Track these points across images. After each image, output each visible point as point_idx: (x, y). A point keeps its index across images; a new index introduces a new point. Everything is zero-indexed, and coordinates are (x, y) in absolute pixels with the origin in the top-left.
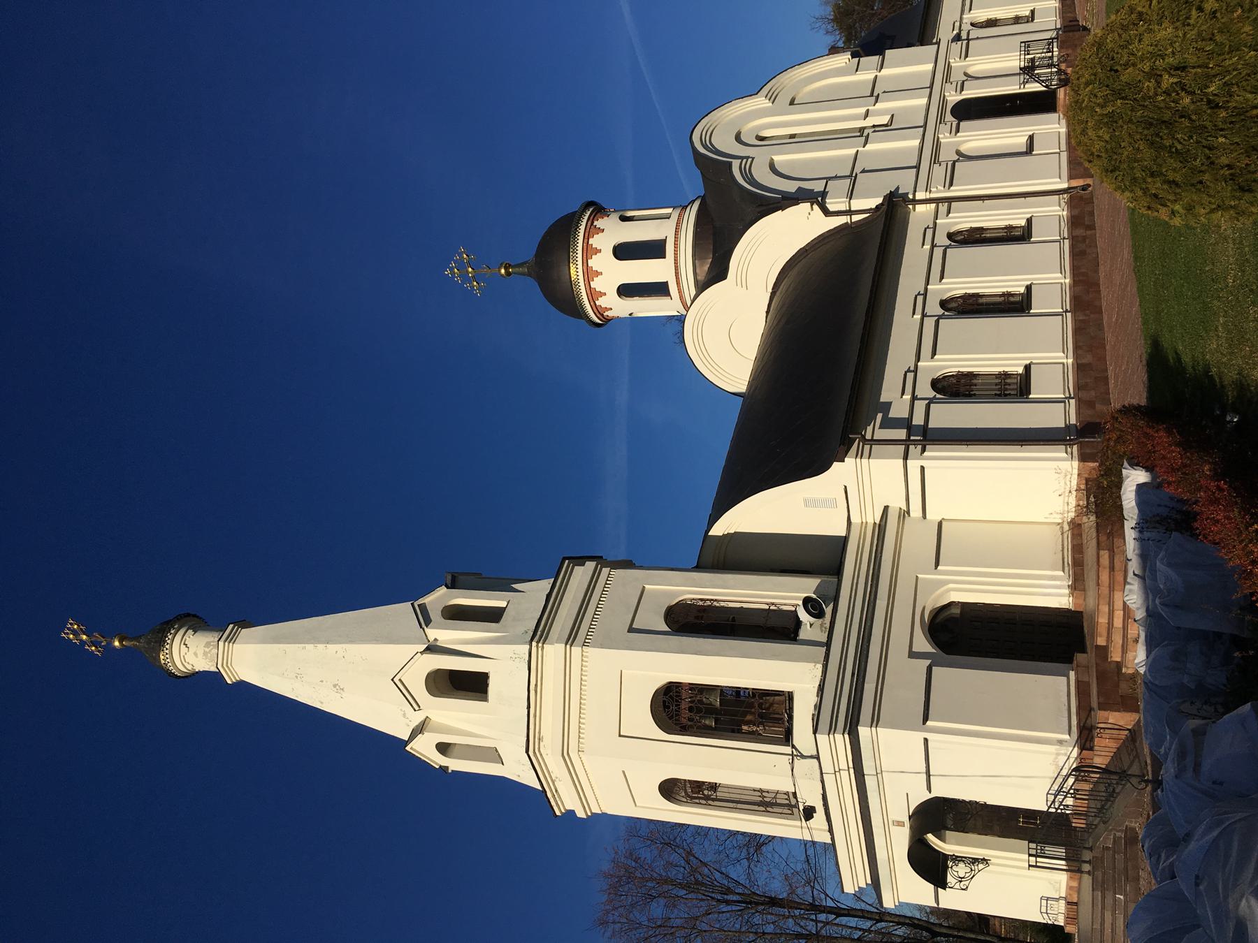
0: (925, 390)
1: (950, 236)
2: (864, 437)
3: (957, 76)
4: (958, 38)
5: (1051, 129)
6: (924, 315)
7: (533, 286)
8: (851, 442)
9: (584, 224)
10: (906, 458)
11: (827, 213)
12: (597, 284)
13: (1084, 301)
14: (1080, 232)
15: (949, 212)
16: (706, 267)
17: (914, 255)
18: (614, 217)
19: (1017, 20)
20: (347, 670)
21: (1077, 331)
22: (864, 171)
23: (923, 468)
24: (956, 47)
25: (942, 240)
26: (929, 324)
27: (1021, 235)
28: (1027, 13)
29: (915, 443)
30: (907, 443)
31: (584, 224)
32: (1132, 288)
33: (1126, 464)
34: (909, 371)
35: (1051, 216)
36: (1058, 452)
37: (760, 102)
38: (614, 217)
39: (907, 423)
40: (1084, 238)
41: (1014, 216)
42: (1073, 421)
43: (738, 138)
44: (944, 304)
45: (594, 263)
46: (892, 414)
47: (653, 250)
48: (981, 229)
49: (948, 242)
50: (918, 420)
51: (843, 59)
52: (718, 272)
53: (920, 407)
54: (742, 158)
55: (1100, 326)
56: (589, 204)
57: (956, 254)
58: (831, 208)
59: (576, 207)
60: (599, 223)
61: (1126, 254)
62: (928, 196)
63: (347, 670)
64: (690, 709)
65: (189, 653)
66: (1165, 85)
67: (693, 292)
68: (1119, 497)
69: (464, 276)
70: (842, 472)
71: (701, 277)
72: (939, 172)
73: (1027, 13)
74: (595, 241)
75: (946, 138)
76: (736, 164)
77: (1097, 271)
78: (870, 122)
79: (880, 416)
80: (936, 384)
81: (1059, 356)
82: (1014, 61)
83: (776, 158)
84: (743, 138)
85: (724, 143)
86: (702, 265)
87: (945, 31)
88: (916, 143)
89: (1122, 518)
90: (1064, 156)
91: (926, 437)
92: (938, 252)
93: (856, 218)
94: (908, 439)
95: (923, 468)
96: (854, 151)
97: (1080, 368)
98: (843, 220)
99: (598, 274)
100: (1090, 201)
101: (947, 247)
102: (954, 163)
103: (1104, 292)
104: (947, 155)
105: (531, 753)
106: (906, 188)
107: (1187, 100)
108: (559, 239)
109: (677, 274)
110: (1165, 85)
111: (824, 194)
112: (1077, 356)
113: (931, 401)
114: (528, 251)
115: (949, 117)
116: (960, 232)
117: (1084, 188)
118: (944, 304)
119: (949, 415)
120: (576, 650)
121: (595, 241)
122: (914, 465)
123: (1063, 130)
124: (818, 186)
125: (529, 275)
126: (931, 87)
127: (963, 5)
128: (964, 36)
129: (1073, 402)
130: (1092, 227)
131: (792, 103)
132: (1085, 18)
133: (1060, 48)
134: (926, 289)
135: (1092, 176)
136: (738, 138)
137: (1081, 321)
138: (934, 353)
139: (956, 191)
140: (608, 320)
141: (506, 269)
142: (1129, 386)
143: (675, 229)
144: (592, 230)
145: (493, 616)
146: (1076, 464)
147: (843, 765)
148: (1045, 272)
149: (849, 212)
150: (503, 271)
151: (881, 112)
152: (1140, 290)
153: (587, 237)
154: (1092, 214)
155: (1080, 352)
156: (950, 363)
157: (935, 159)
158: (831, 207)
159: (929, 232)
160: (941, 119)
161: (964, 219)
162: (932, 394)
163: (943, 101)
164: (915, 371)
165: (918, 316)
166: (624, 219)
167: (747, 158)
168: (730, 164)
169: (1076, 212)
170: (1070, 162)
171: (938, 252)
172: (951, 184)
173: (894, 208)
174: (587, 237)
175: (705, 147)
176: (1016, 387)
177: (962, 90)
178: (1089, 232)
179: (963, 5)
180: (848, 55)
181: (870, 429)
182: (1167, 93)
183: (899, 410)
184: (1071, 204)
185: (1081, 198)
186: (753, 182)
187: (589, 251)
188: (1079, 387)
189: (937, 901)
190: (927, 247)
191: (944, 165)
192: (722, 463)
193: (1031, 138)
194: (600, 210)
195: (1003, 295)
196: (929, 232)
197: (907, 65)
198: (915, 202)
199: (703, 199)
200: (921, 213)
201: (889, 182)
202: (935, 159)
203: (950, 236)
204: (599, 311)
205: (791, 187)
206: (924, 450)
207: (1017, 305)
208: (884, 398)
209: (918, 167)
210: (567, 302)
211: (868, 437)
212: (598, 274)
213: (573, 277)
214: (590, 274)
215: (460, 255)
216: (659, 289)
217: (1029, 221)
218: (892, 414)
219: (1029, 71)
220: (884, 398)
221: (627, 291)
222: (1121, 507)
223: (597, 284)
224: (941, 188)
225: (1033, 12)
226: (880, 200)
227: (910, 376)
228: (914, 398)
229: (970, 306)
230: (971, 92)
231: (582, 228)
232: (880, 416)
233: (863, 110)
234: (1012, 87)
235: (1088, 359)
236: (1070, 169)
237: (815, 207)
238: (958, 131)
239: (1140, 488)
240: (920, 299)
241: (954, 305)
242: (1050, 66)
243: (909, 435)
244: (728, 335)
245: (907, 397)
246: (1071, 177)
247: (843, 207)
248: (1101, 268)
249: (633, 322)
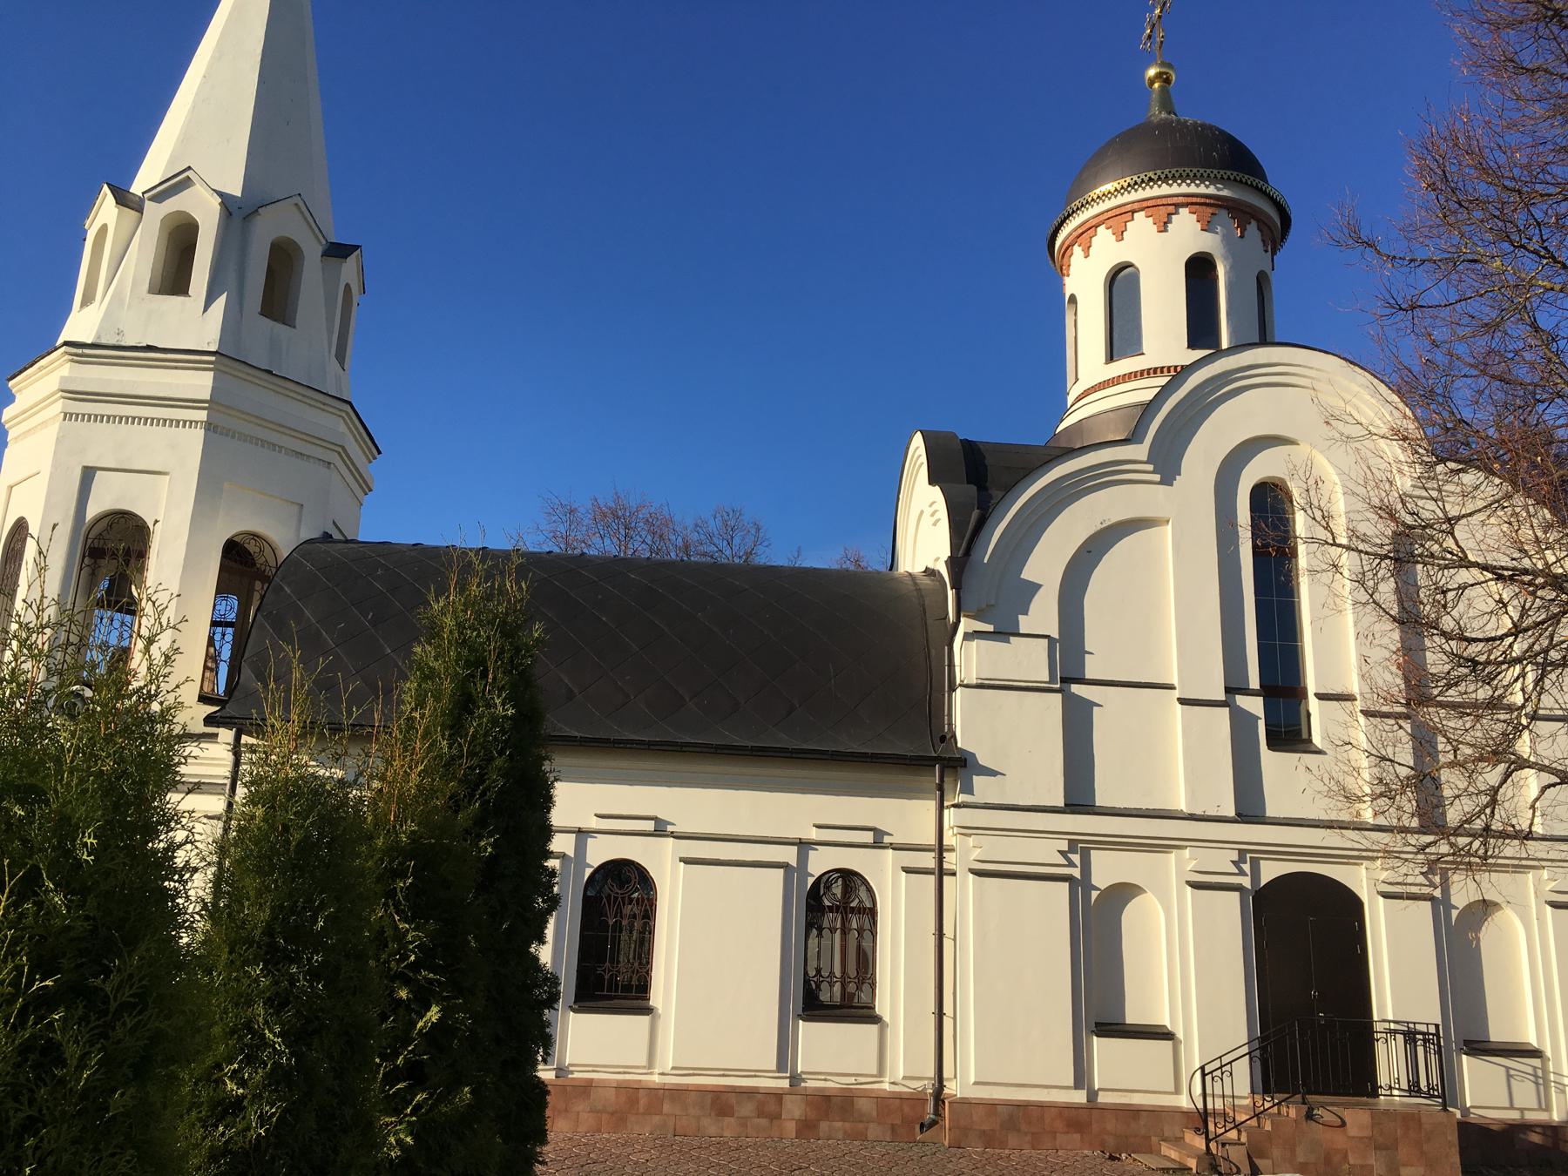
9: (1175, 189)
14: (794, 1109)
31: (1175, 189)
40: (775, 1117)
45: (1104, 235)
72: (1047, 852)
74: (1142, 224)
76: (1140, 451)
83: (1169, 527)
92: (789, 855)
96: (1175, 682)
111: (1004, 633)
115: (1270, 871)
120: (58, 407)
121: (1142, 224)
144: (1163, 213)
145: (173, 279)
153: (1147, 206)
159: (868, 837)
169: (863, 1105)
173: (941, 764)
174: (1147, 206)
177: (1386, 896)
178: (790, 1128)
184: (916, 1099)
198: (941, 808)
200: (910, 817)
205: (1046, 564)
224: (976, 854)
231: (1165, 190)
233: (1354, 686)
236: (991, 1106)
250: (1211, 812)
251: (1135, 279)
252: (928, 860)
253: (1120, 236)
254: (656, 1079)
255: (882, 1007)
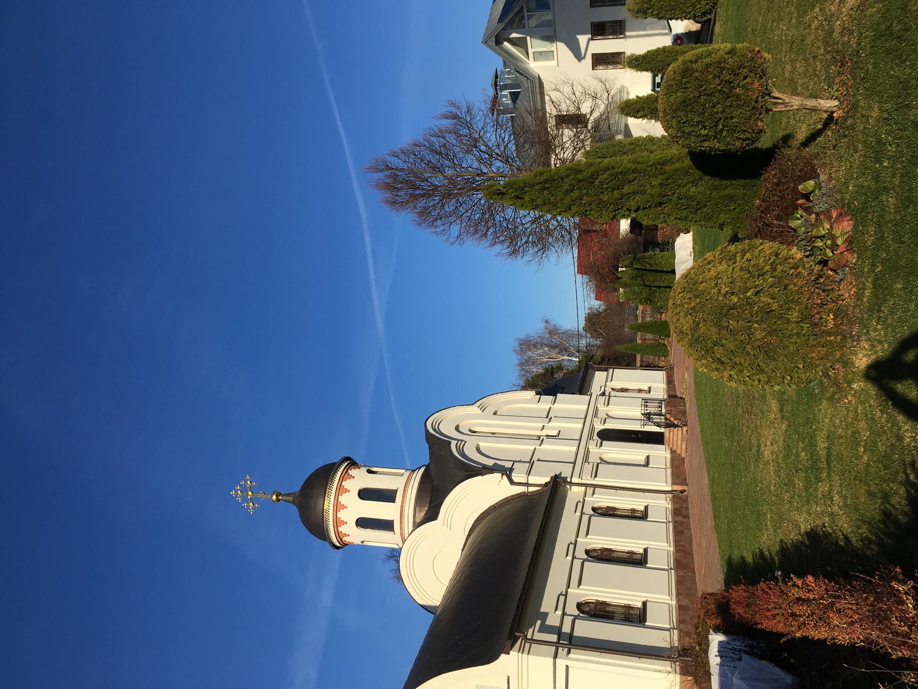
0: (572, 609)
1: (594, 509)
2: (526, 636)
3: (602, 415)
4: (603, 394)
5: (660, 454)
6: (574, 558)
7: (294, 510)
8: (519, 638)
9: (341, 471)
10: (555, 657)
11: (512, 482)
12: (342, 515)
13: (683, 562)
14: (680, 519)
15: (594, 494)
16: (423, 513)
17: (569, 519)
18: (363, 470)
19: (640, 391)
21: (680, 582)
22: (539, 460)
23: (567, 667)
24: (602, 399)
25: (588, 510)
26: (577, 563)
27: (643, 516)
28: (646, 388)
29: (563, 646)
30: (557, 645)
31: (342, 469)
32: (715, 543)
33: (711, 631)
34: (561, 594)
35: (661, 506)
36: (666, 666)
37: (474, 409)
38: (363, 470)
39: (558, 631)
40: (682, 523)
41: (637, 503)
42: (676, 644)
43: (457, 428)
44: (587, 552)
45: (343, 499)
46: (549, 622)
47: (387, 496)
48: (614, 509)
49: (592, 513)
50: (566, 629)
51: (530, 394)
52: (432, 515)
53: (568, 621)
54: (458, 440)
55: (694, 582)
56: (347, 459)
57: (596, 520)
58: (515, 479)
59: (337, 460)
60: (352, 472)
61: (710, 522)
62: (580, 481)
66: (723, 292)
67: (411, 528)
68: (708, 657)
69: (244, 498)
70: (508, 662)
71: (418, 520)
72: (588, 468)
73: (646, 388)
74: (346, 484)
75: (593, 448)
76: (453, 443)
77: (691, 545)
78: (545, 432)
79: (539, 623)
80: (579, 606)
81: (666, 598)
82: (636, 411)
83: (481, 444)
84: (460, 429)
85: (447, 429)
86: (420, 511)
87: (595, 389)
88: (574, 449)
89: (708, 674)
90: (669, 471)
91: (570, 642)
92: (585, 518)
93: (531, 489)
94: (558, 642)
95: (567, 667)
96: (533, 448)
97: (681, 608)
98: (522, 489)
99: (344, 507)
100: (686, 500)
101: (591, 515)
102: (598, 464)
103: (696, 557)
104: (594, 459)
106: (566, 473)
107: (736, 300)
108: (321, 478)
109: (401, 519)
110: (723, 292)
111: (511, 470)
112: (678, 600)
113: (576, 618)
114: (297, 487)
116: (600, 508)
117: (682, 492)
118: (587, 552)
119: (588, 629)
122: (561, 663)
123: (668, 456)
124: (508, 465)
125: (293, 503)
126: (585, 418)
127: (607, 378)
128: (607, 394)
129: (676, 631)
130: (687, 517)
131: (495, 414)
132: (682, 393)
133: (666, 406)
134: (576, 541)
135: (687, 485)
136: (457, 428)
137: (682, 577)
138: (580, 584)
139: (598, 481)
140: (345, 545)
141: (277, 495)
142: (711, 579)
143: (405, 483)
146: (677, 678)
148: (656, 540)
149: (527, 484)
150: (274, 497)
151: (552, 428)
152: (717, 527)
153: (342, 479)
154: (687, 509)
155: (680, 597)
156: (591, 592)
157: (586, 459)
158: (515, 479)
159: (580, 505)
160: (590, 437)
161: (604, 500)
162: (577, 612)
163: (592, 428)
164: (566, 595)
165: (570, 558)
166: (370, 472)
167: (462, 441)
168: (450, 443)
169: (676, 506)
170: (673, 474)
171: (585, 518)
172: (596, 476)
173: (557, 485)
174: (342, 479)
175: (434, 430)
176: (635, 616)
179: (607, 378)
180: (534, 393)
181: (531, 630)
182: (725, 295)
183: (553, 620)
185: (680, 498)
186: (463, 455)
187: (341, 490)
188: (681, 621)
190: (578, 514)
191: (591, 465)
192: (415, 653)
193: (648, 457)
194: (353, 464)
195: (629, 552)
196: (580, 505)
197: (570, 404)
198: (571, 483)
199: (428, 467)
200: (574, 493)
201: (556, 469)
202: (586, 459)
203: (594, 509)
204: (339, 535)
205: (490, 463)
206: (569, 652)
207: (638, 560)
208: (543, 610)
209: (574, 463)
210: (317, 528)
211: (529, 637)
212: (344, 507)
213: (326, 506)
214: (338, 507)
215: (246, 481)
216: (387, 525)
217: (646, 508)
218: (549, 622)
219: (648, 416)
220: (543, 610)
221: (363, 523)
222: (708, 663)
223: (342, 515)
225: (650, 388)
226: (548, 479)
227: (562, 598)
228: (564, 614)
229: (605, 556)
230: (611, 425)
231: (339, 473)
232: (539, 623)
233: (541, 425)
234: (636, 427)
235: (686, 602)
236: (673, 479)
237: (505, 477)
238: (601, 445)
239: (720, 642)
240: (572, 547)
241: (594, 554)
242: (660, 415)
243: (559, 639)
244: (432, 561)
245: (559, 613)
246: (673, 484)
247: (524, 480)
248: (694, 542)
249: (363, 549)
250: (580, 433)
251: (364, 489)
252: (590, 490)
253: (347, 491)
254: (672, 549)
255: (642, 508)
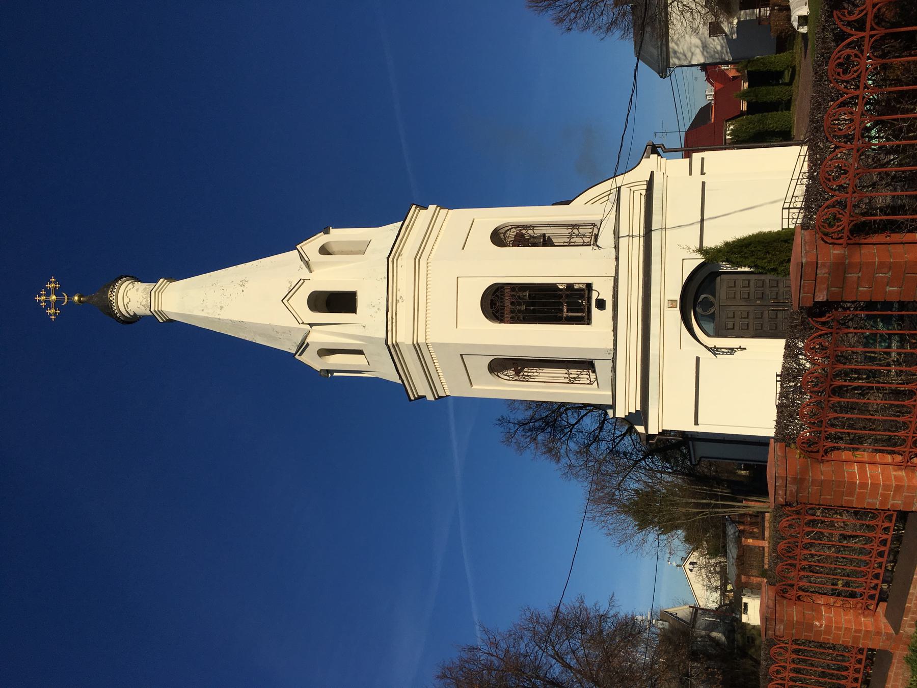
20: (245, 299)
23: (703, 159)
63: (245, 299)
64: (512, 303)
65: (131, 297)
95: (703, 159)
105: (390, 259)
147: (636, 232)
189: (696, 423)
